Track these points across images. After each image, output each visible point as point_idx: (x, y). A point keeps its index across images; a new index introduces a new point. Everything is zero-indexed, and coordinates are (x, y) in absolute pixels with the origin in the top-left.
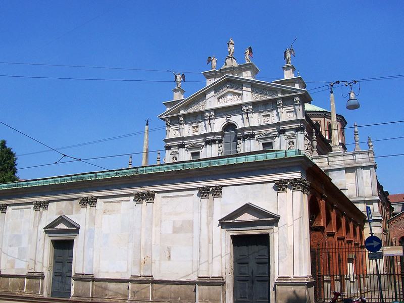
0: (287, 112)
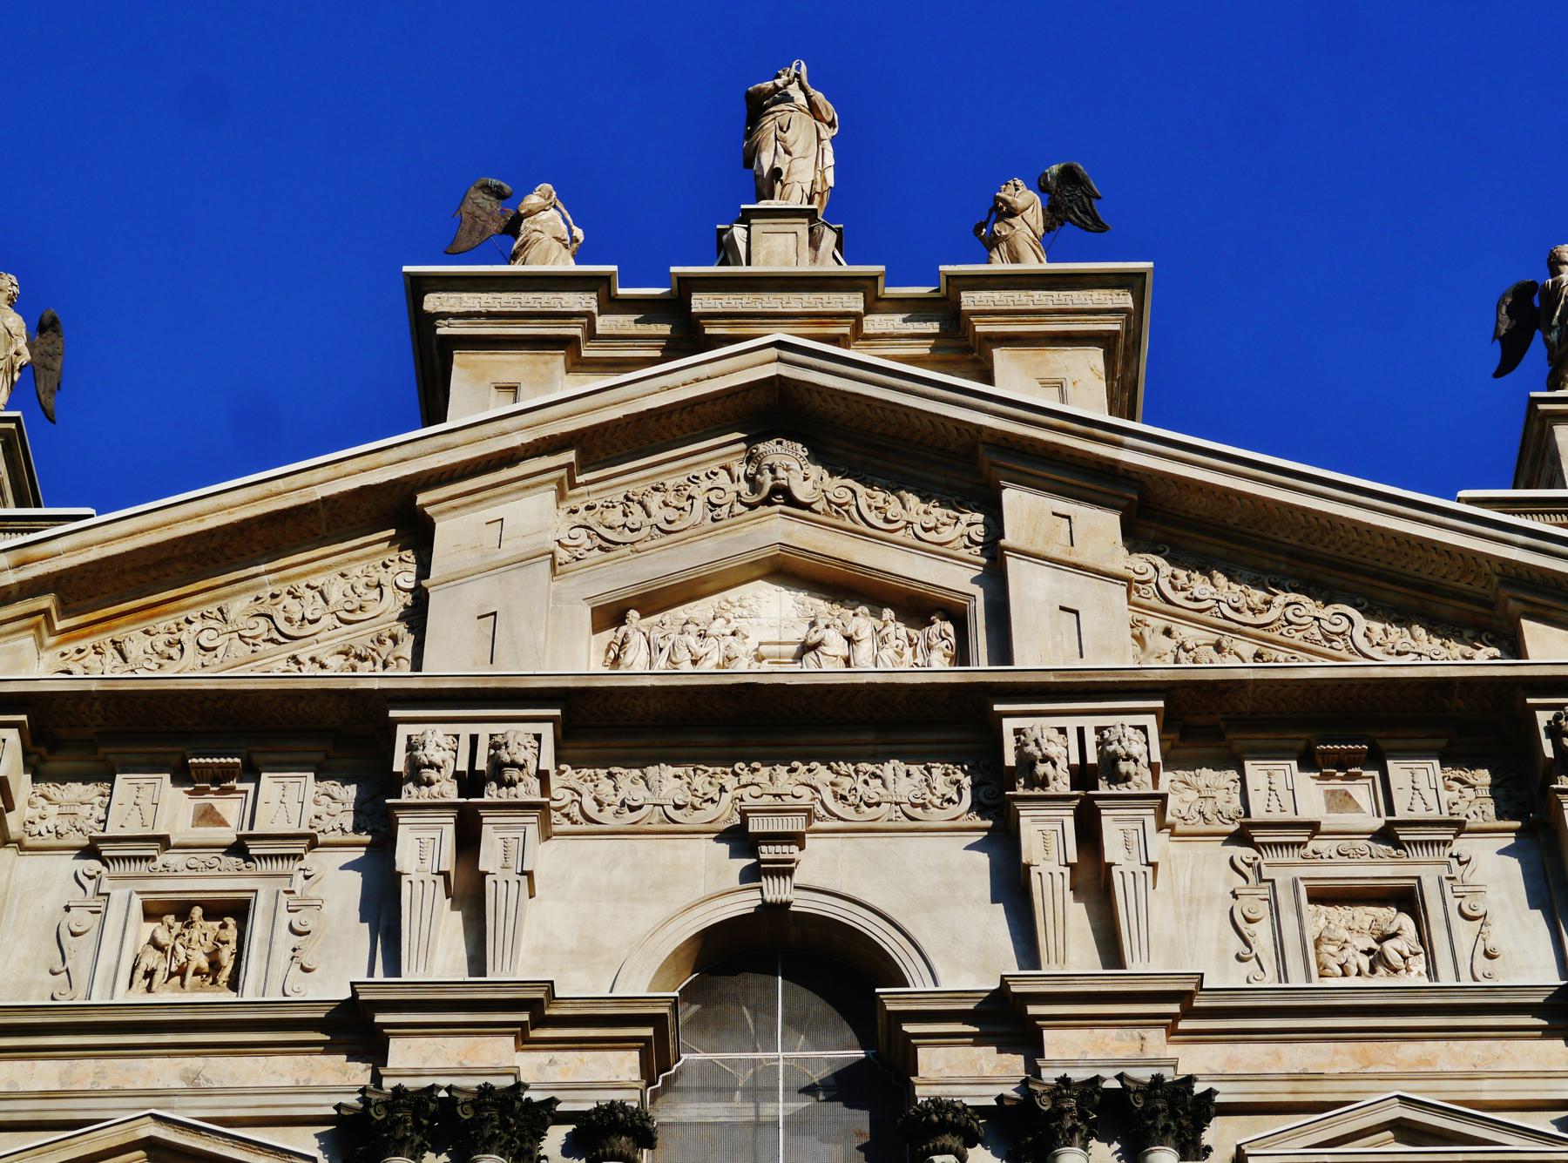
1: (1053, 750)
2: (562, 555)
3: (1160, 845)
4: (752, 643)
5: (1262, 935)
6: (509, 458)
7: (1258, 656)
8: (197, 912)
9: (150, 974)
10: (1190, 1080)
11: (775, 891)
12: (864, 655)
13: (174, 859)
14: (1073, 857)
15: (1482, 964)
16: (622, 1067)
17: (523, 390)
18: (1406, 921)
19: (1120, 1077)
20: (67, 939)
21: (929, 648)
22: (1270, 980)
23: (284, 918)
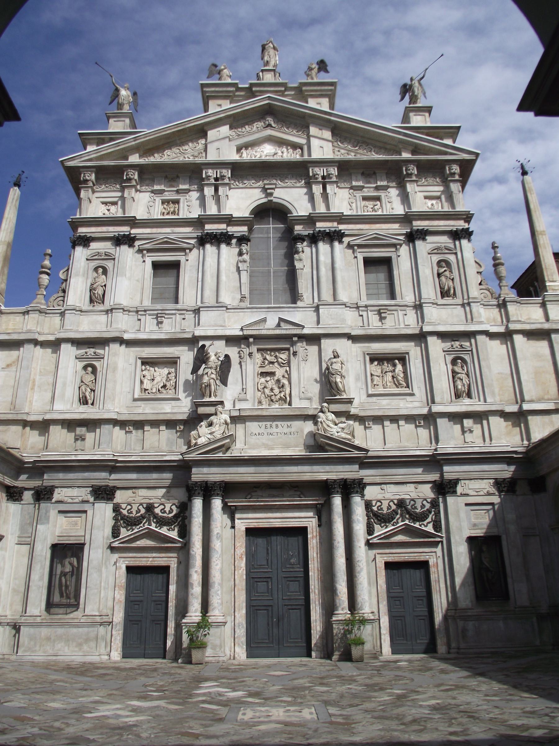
0: (426, 198)
1: (318, 173)
2: (231, 137)
3: (337, 190)
4: (265, 153)
5: (354, 205)
7: (355, 156)
8: (171, 202)
9: (164, 213)
10: (341, 230)
12: (285, 155)
14: (322, 192)
15: (391, 210)
16: (245, 229)
17: (223, 106)
18: (378, 203)
19: (329, 230)
20: (149, 207)
21: (297, 154)
22: (355, 213)
23: (186, 204)
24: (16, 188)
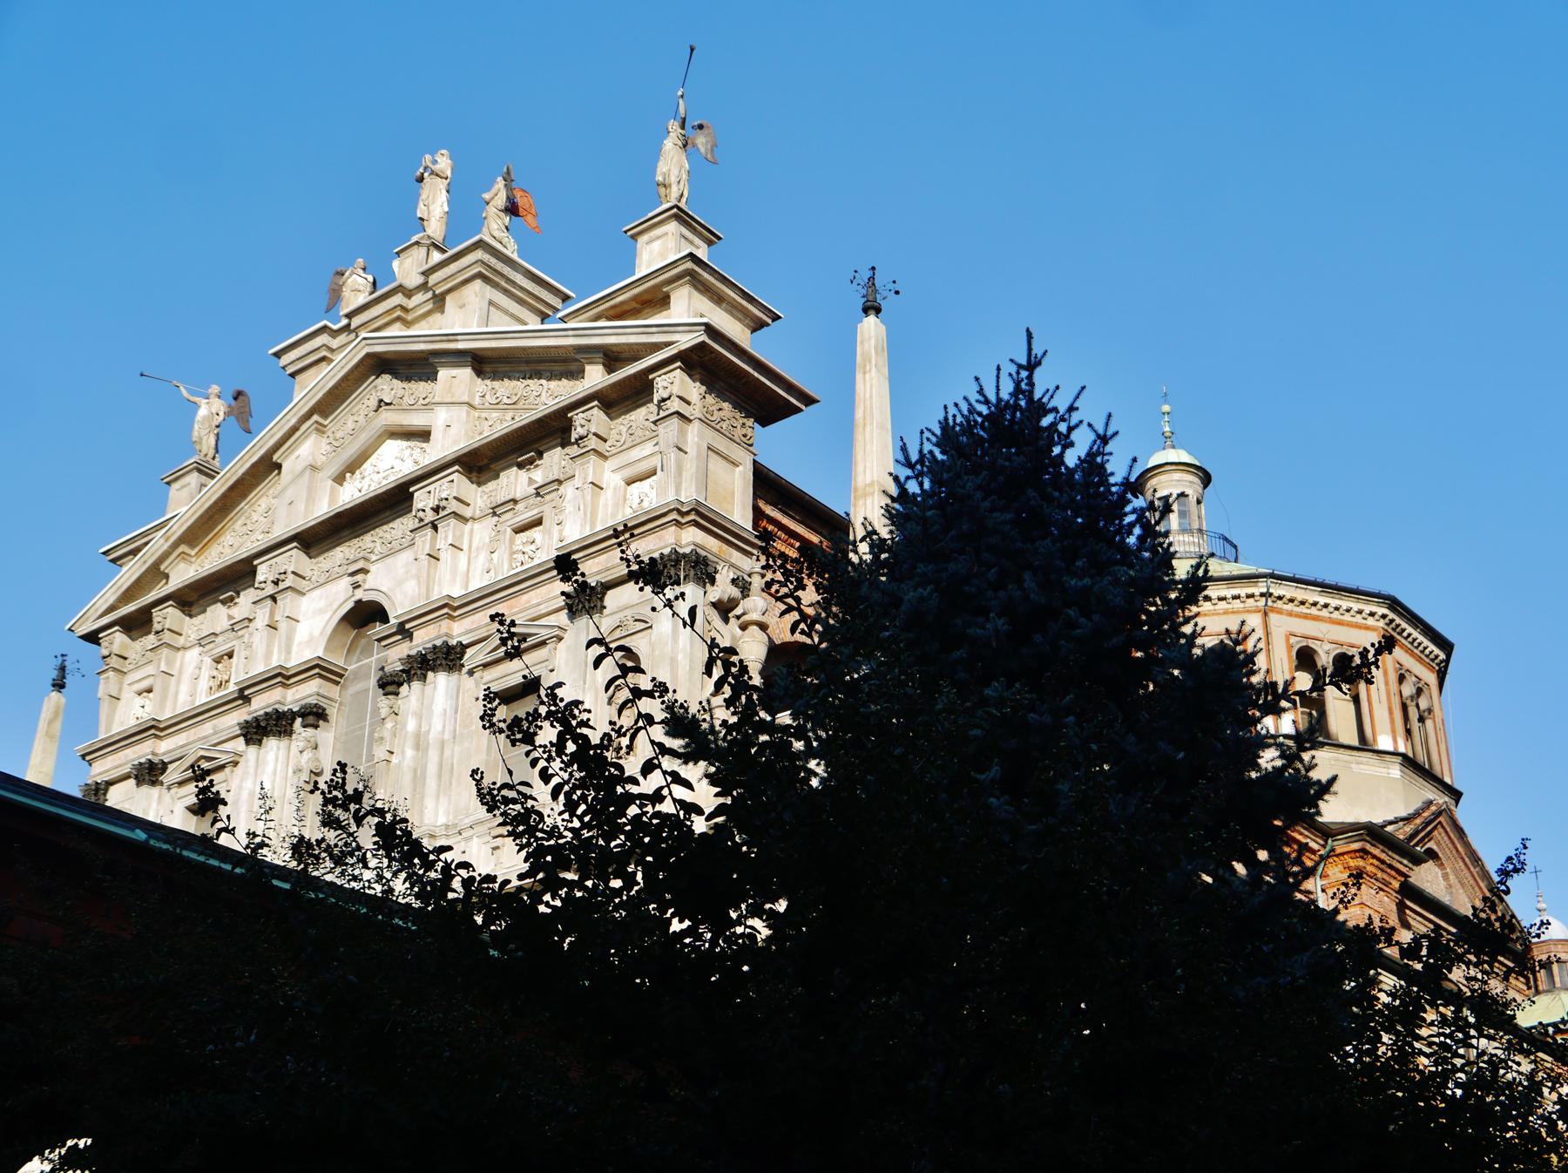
0: (629, 483)
6: (294, 429)
11: (360, 594)
13: (220, 639)
19: (424, 649)
24: (872, 319)
